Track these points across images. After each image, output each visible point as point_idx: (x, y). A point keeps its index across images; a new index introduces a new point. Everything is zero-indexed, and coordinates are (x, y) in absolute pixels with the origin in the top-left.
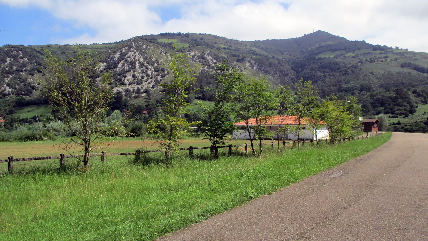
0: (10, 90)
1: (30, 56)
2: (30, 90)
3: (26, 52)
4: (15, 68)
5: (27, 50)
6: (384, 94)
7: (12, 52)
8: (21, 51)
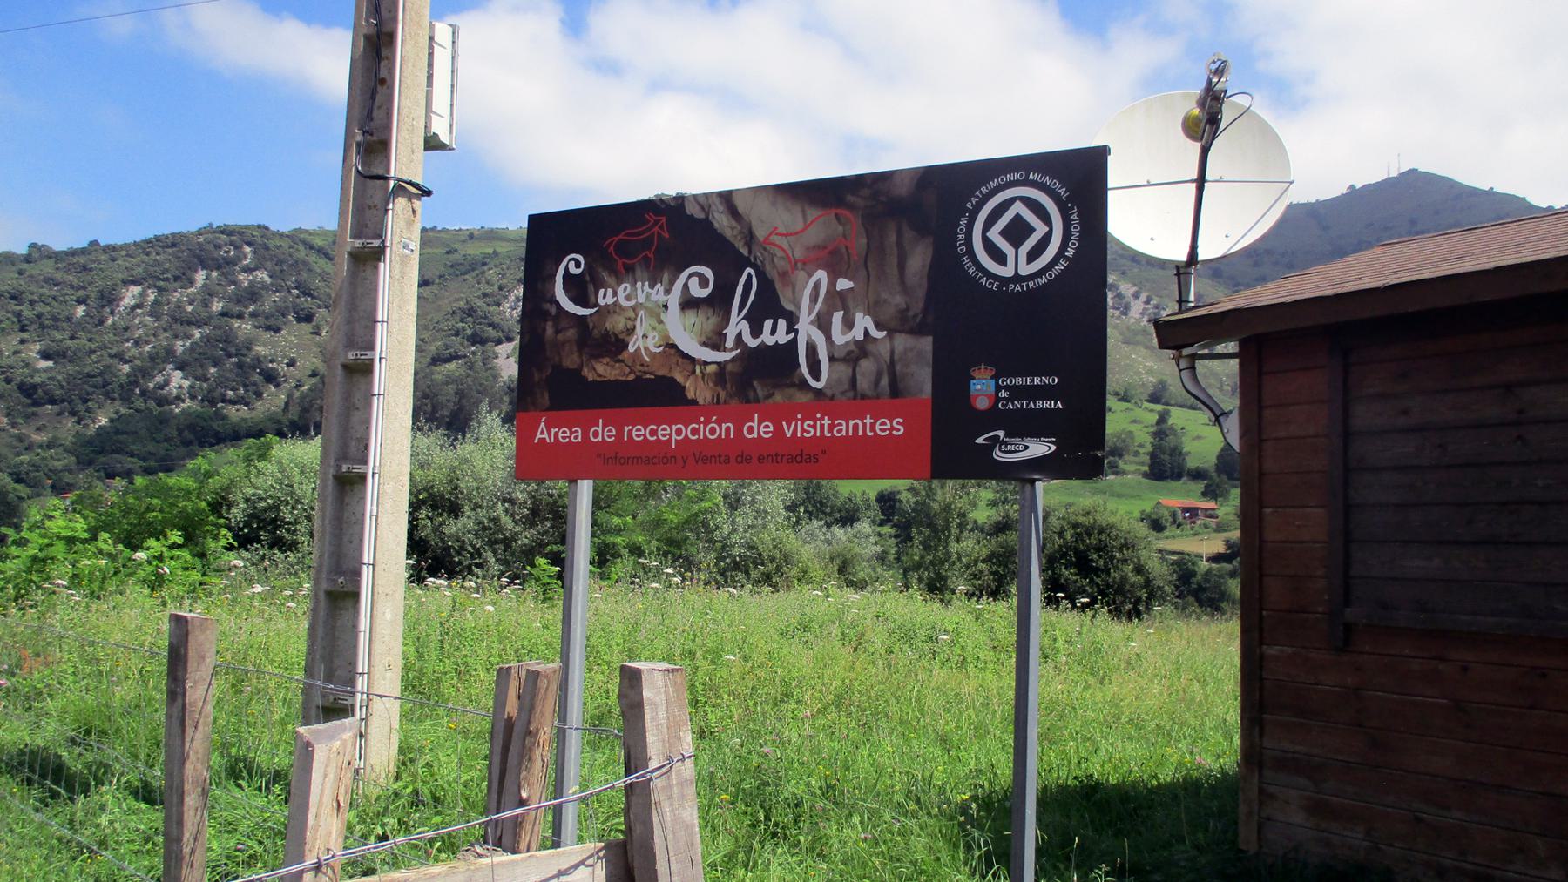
0: (186, 383)
1: (280, 262)
2: (255, 384)
3: (267, 248)
4: (217, 306)
5: (271, 244)
6: (198, 858)
7: (218, 247)
8: (249, 244)
